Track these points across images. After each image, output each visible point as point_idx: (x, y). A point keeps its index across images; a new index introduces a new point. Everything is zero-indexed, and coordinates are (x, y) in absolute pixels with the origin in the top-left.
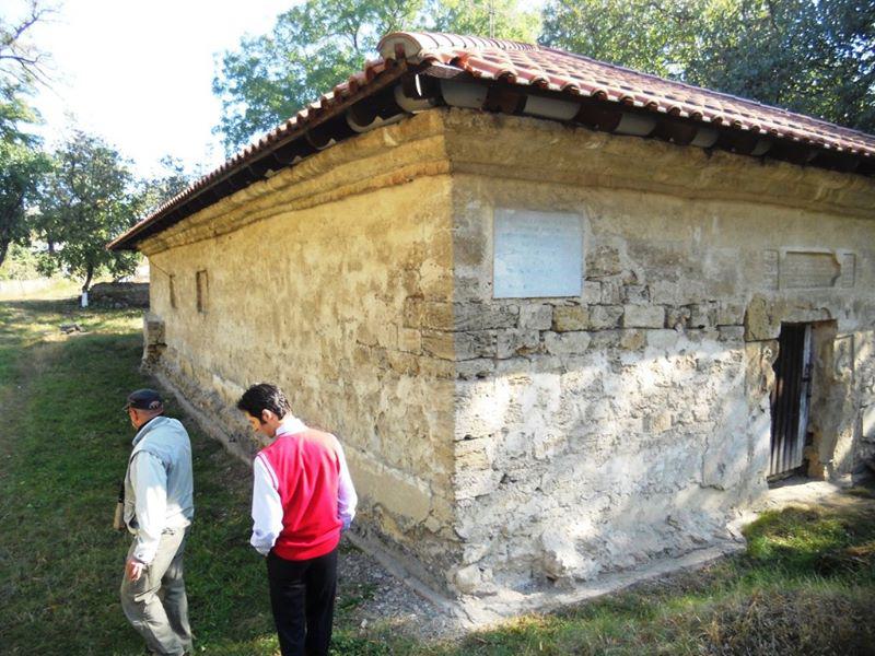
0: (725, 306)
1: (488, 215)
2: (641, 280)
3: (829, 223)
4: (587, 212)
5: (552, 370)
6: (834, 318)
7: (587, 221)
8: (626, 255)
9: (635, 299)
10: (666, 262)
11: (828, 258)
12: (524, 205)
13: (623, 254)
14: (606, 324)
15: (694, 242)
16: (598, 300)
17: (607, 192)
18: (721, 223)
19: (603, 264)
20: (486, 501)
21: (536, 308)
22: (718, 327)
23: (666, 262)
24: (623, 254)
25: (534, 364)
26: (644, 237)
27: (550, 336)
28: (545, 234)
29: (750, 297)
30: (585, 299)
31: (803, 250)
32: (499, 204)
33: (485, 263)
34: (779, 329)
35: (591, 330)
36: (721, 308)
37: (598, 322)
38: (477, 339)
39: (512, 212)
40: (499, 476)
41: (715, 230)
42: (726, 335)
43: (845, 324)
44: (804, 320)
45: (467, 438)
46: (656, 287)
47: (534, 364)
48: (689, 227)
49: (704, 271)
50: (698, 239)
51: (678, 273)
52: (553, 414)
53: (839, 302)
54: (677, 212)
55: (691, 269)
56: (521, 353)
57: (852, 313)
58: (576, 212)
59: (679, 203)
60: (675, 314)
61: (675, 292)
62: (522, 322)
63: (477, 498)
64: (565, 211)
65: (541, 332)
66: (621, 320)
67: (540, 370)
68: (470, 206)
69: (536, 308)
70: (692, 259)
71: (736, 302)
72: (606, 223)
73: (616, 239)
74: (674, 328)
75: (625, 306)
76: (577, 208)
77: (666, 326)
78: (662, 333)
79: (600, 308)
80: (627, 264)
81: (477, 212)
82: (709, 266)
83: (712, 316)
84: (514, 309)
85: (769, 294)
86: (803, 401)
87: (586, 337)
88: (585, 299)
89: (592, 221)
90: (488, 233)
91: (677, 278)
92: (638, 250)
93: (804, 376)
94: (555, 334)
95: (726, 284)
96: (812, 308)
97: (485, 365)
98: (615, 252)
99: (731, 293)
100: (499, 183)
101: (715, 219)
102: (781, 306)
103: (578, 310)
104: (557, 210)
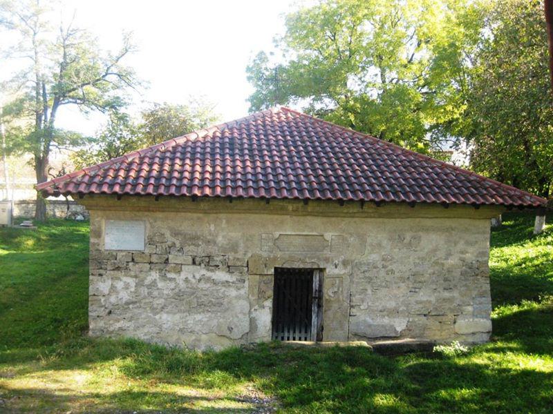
0: (231, 258)
1: (103, 222)
2: (178, 245)
3: (317, 221)
4: (149, 221)
5: (131, 277)
6: (321, 267)
7: (148, 223)
8: (169, 236)
9: (174, 252)
10: (194, 239)
11: (320, 237)
12: (120, 219)
13: (168, 234)
14: (159, 261)
15: (210, 230)
16: (154, 252)
17: (158, 213)
18: (228, 222)
19: (157, 239)
20: (102, 318)
21: (124, 254)
22: (229, 267)
23: (194, 239)
24: (168, 234)
25: (123, 273)
26: (180, 229)
27: (131, 264)
28: (127, 228)
29: (249, 255)
30: (147, 251)
31: (293, 233)
32: (108, 218)
33: (102, 238)
34: (273, 270)
35: (150, 263)
36: (228, 258)
37: (154, 259)
38: (100, 263)
39: (112, 221)
40: (107, 311)
41: (224, 224)
42: (233, 271)
43: (330, 270)
44: (309, 266)
45: (94, 295)
46: (186, 249)
47: (123, 273)
48: (207, 224)
49: (217, 242)
50: (213, 229)
51: (200, 243)
52: (131, 292)
53: (327, 260)
54: (199, 218)
55: (209, 242)
56: (118, 269)
57: (340, 266)
58: (141, 220)
59: (201, 215)
60: (198, 260)
61: (200, 251)
62: (118, 258)
63: (98, 316)
64: (136, 220)
65: (128, 262)
66: (167, 259)
67: (126, 276)
68: (97, 219)
69: (124, 254)
70: (208, 237)
71: (239, 255)
72: (159, 223)
73: (163, 230)
74: (200, 264)
75: (170, 256)
76: (144, 219)
77: (194, 263)
78: (192, 267)
79: (155, 255)
80: (170, 239)
81: (99, 221)
82: (220, 239)
83: (224, 262)
84: (114, 254)
85: (265, 254)
86: (315, 308)
87: (148, 266)
88: (147, 251)
89: (150, 223)
90: (103, 228)
91: (199, 245)
92: (176, 234)
93: (314, 296)
94: (132, 263)
95: (234, 248)
96: (303, 262)
97: (102, 271)
98: (163, 234)
99: (236, 252)
100: (108, 212)
101: (224, 221)
102: (275, 259)
103: (143, 255)
104: (133, 220)
